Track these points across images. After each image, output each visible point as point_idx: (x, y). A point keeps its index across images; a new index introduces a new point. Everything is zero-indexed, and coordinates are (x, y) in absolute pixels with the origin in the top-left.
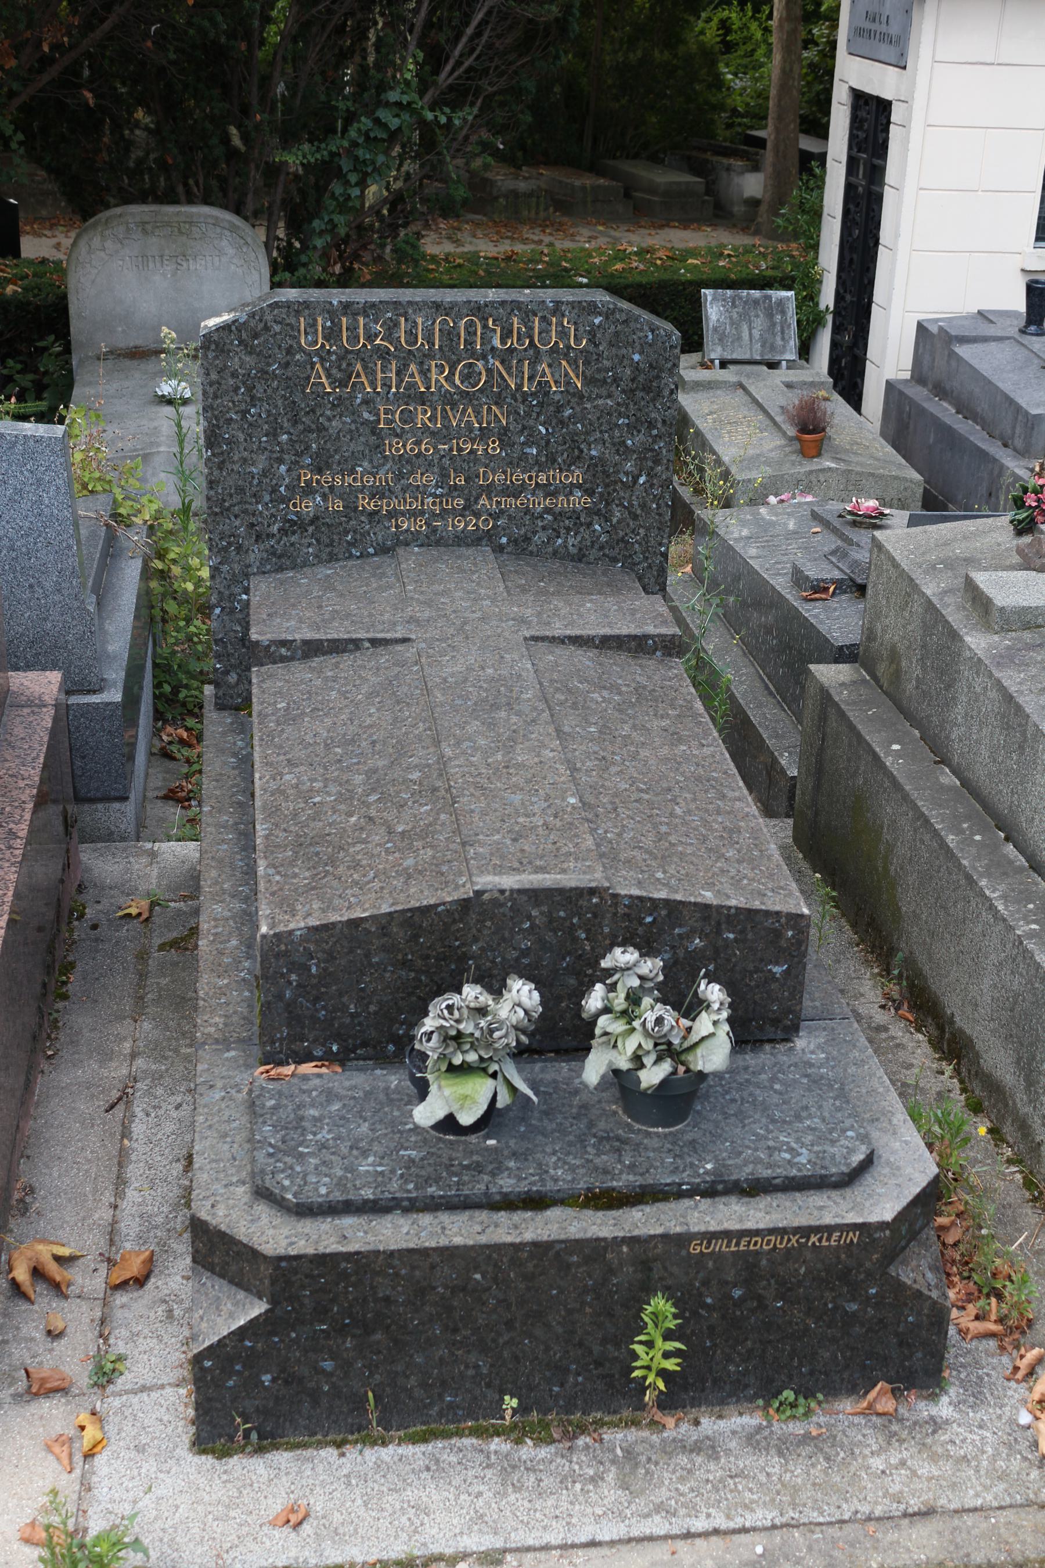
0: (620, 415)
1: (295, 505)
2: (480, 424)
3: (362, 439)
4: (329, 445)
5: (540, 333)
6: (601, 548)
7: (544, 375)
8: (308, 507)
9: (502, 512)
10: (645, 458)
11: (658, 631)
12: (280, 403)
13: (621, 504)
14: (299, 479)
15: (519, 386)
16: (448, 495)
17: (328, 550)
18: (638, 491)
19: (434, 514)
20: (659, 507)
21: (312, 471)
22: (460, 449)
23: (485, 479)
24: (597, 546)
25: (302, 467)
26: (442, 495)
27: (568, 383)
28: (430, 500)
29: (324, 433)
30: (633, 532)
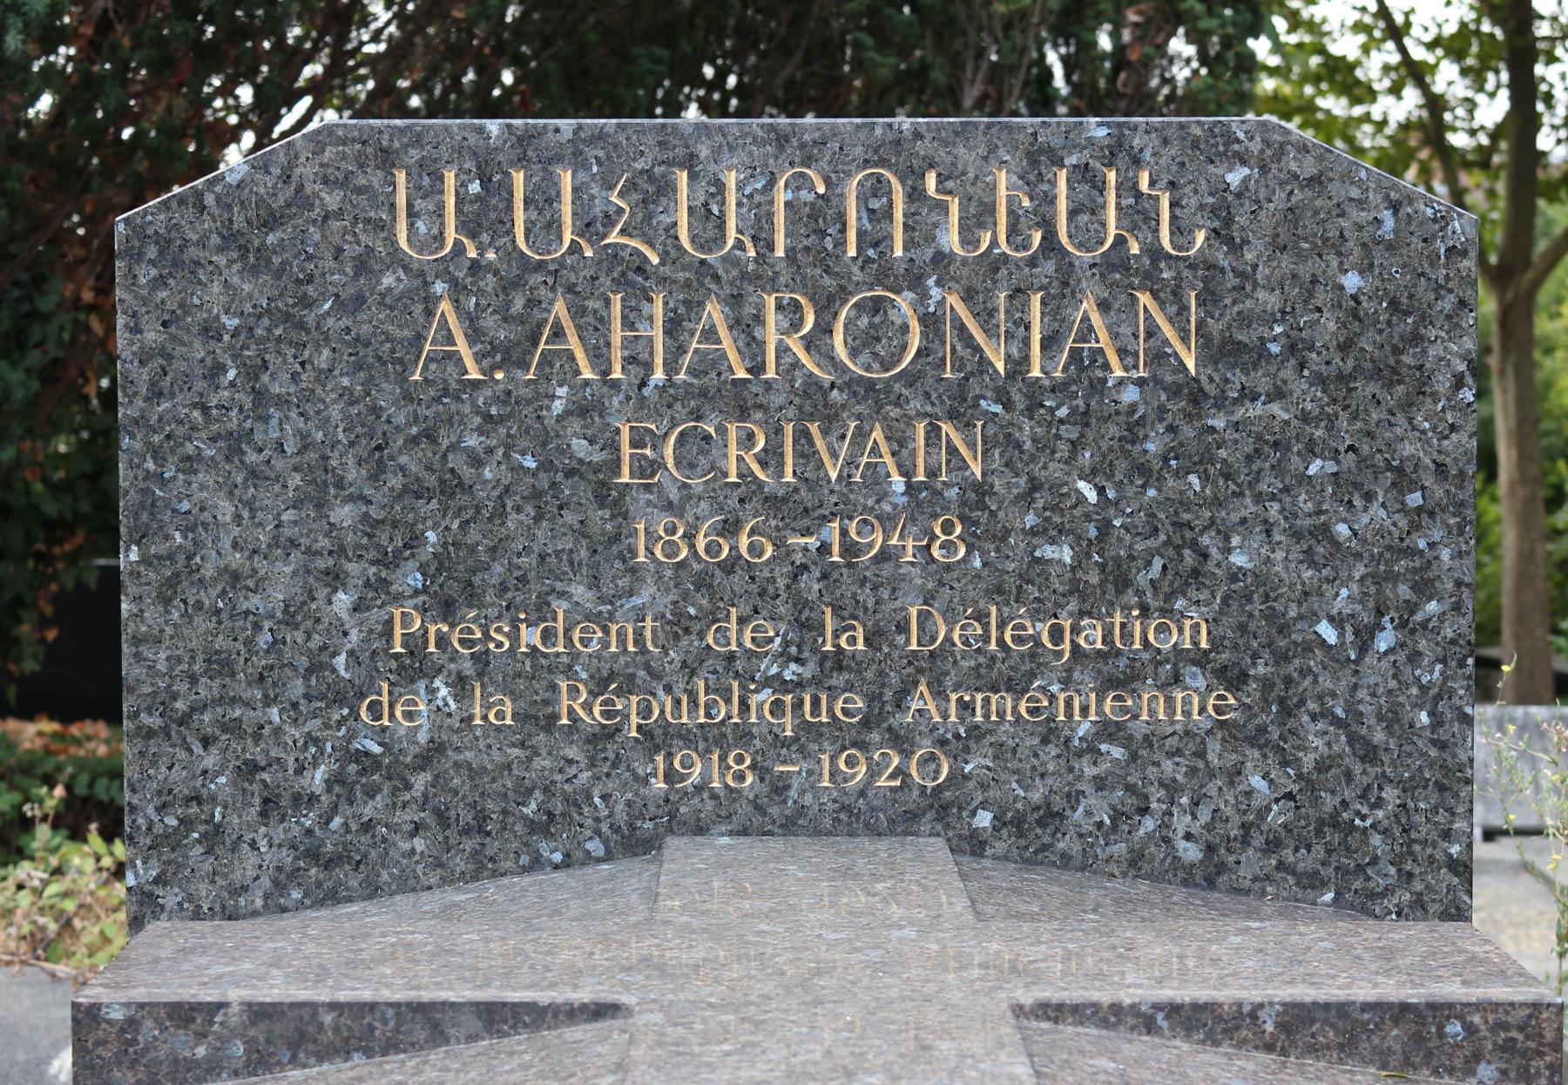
0: (1311, 451)
1: (375, 708)
2: (907, 473)
3: (570, 518)
4: (474, 535)
5: (1072, 214)
6: (1273, 845)
7: (1087, 331)
8: (416, 715)
9: (976, 733)
10: (1394, 578)
11: (1475, 994)
12: (335, 412)
13: (1325, 714)
14: (388, 633)
15: (1018, 365)
16: (817, 682)
17: (469, 844)
18: (1375, 671)
19: (778, 741)
20: (1437, 722)
21: (424, 610)
22: (850, 549)
23: (927, 635)
24: (1258, 840)
25: (398, 598)
26: (800, 684)
27: (1159, 356)
28: (766, 696)
29: (461, 499)
30: (1363, 797)
